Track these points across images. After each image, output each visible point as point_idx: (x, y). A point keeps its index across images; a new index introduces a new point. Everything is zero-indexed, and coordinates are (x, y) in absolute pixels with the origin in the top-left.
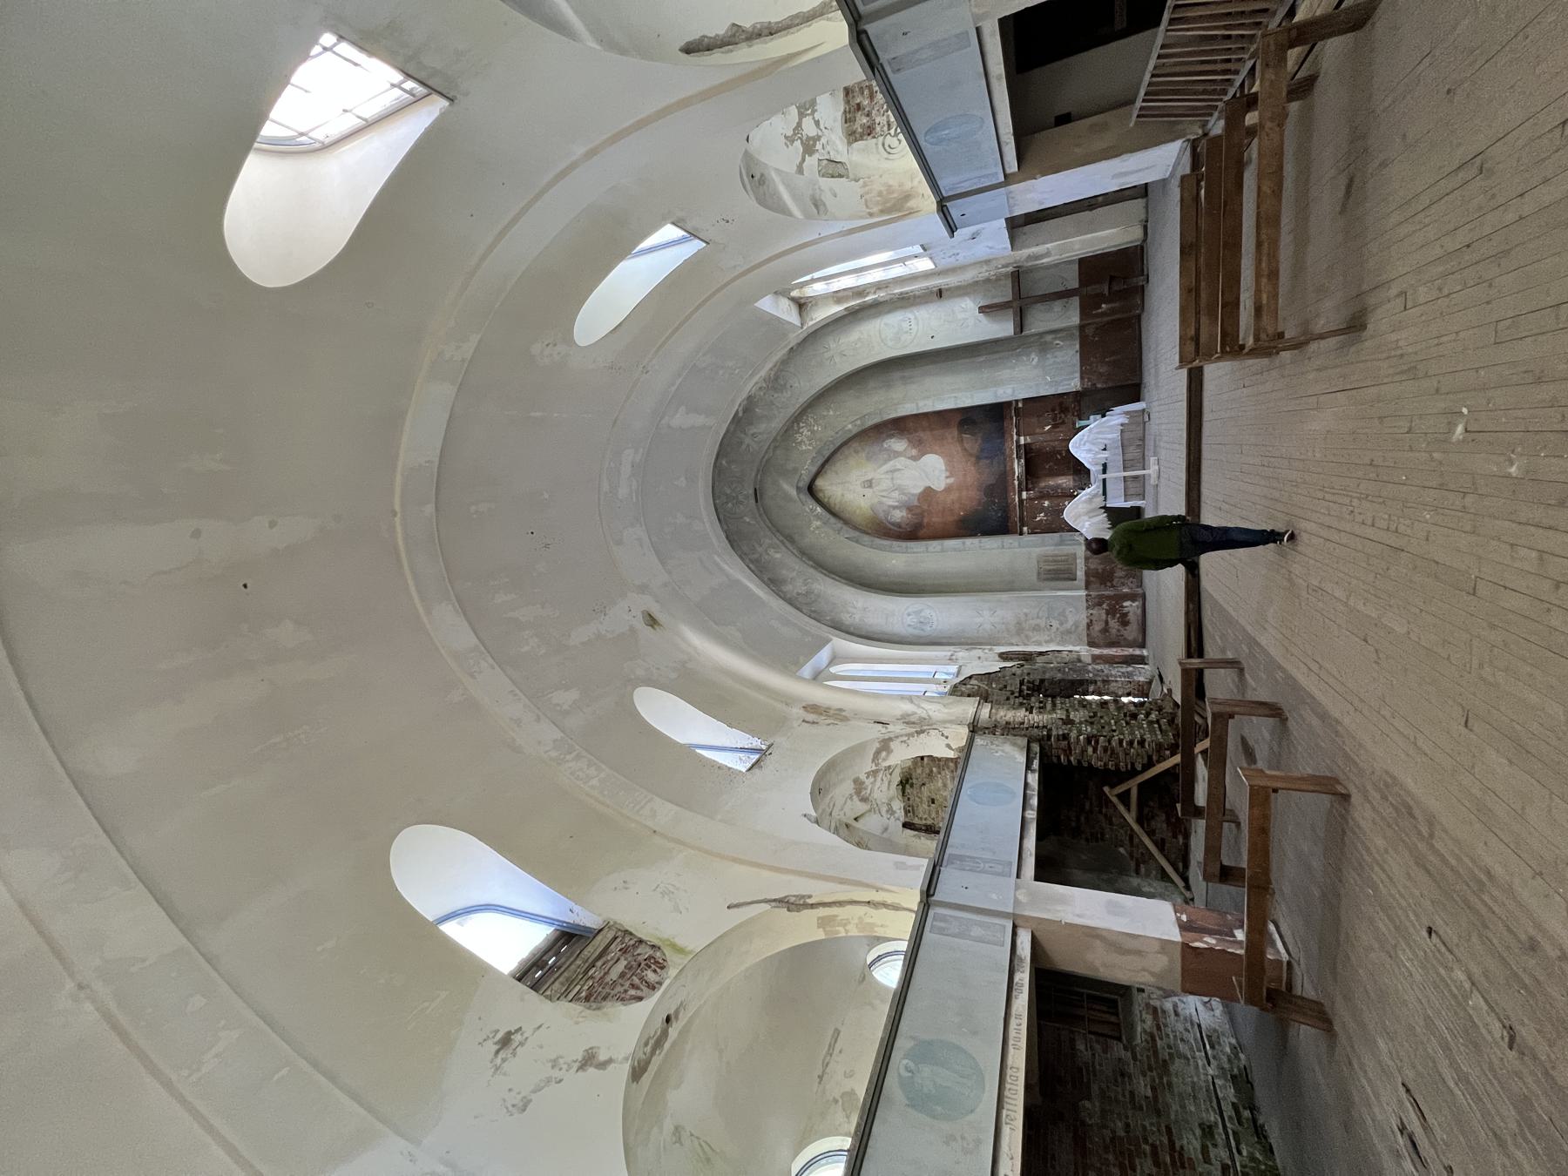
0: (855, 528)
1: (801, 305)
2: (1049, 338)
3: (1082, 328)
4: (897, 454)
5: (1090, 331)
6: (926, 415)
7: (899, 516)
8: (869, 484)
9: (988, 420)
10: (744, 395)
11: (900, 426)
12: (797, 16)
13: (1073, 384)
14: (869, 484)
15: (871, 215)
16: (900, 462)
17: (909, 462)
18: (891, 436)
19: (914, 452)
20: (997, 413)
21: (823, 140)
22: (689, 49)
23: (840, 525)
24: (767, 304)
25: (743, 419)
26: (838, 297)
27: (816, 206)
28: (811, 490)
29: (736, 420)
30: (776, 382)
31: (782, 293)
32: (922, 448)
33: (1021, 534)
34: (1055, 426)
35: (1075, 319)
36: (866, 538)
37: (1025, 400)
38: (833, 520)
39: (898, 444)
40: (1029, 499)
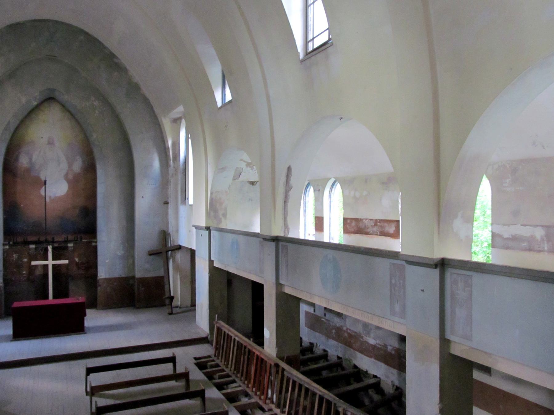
0: (17, 129)
1: (176, 121)
2: (131, 261)
3: (133, 278)
4: (70, 166)
5: (131, 282)
6: (95, 186)
7: (23, 161)
8: (51, 143)
9: (84, 224)
10: (128, 67)
11: (90, 168)
12: (287, 214)
13: (103, 273)
14: (51, 143)
15: (212, 194)
16: (64, 166)
17: (64, 172)
18: (84, 162)
19: (71, 177)
20: (91, 230)
21: (251, 171)
22: (289, 169)
23: (21, 117)
24: (181, 109)
25: (111, 61)
26: (176, 144)
27: (223, 168)
28: (50, 99)
29: (112, 56)
30: (134, 90)
31: (184, 116)
32: (73, 182)
33: (4, 245)
34: (77, 264)
35: (138, 275)
36: (8, 136)
37: (96, 248)
38: (26, 113)
39: (78, 166)
40: (30, 249)
